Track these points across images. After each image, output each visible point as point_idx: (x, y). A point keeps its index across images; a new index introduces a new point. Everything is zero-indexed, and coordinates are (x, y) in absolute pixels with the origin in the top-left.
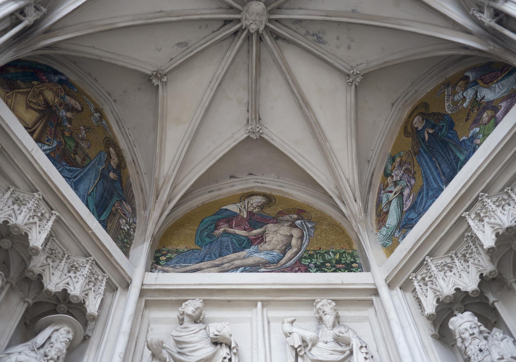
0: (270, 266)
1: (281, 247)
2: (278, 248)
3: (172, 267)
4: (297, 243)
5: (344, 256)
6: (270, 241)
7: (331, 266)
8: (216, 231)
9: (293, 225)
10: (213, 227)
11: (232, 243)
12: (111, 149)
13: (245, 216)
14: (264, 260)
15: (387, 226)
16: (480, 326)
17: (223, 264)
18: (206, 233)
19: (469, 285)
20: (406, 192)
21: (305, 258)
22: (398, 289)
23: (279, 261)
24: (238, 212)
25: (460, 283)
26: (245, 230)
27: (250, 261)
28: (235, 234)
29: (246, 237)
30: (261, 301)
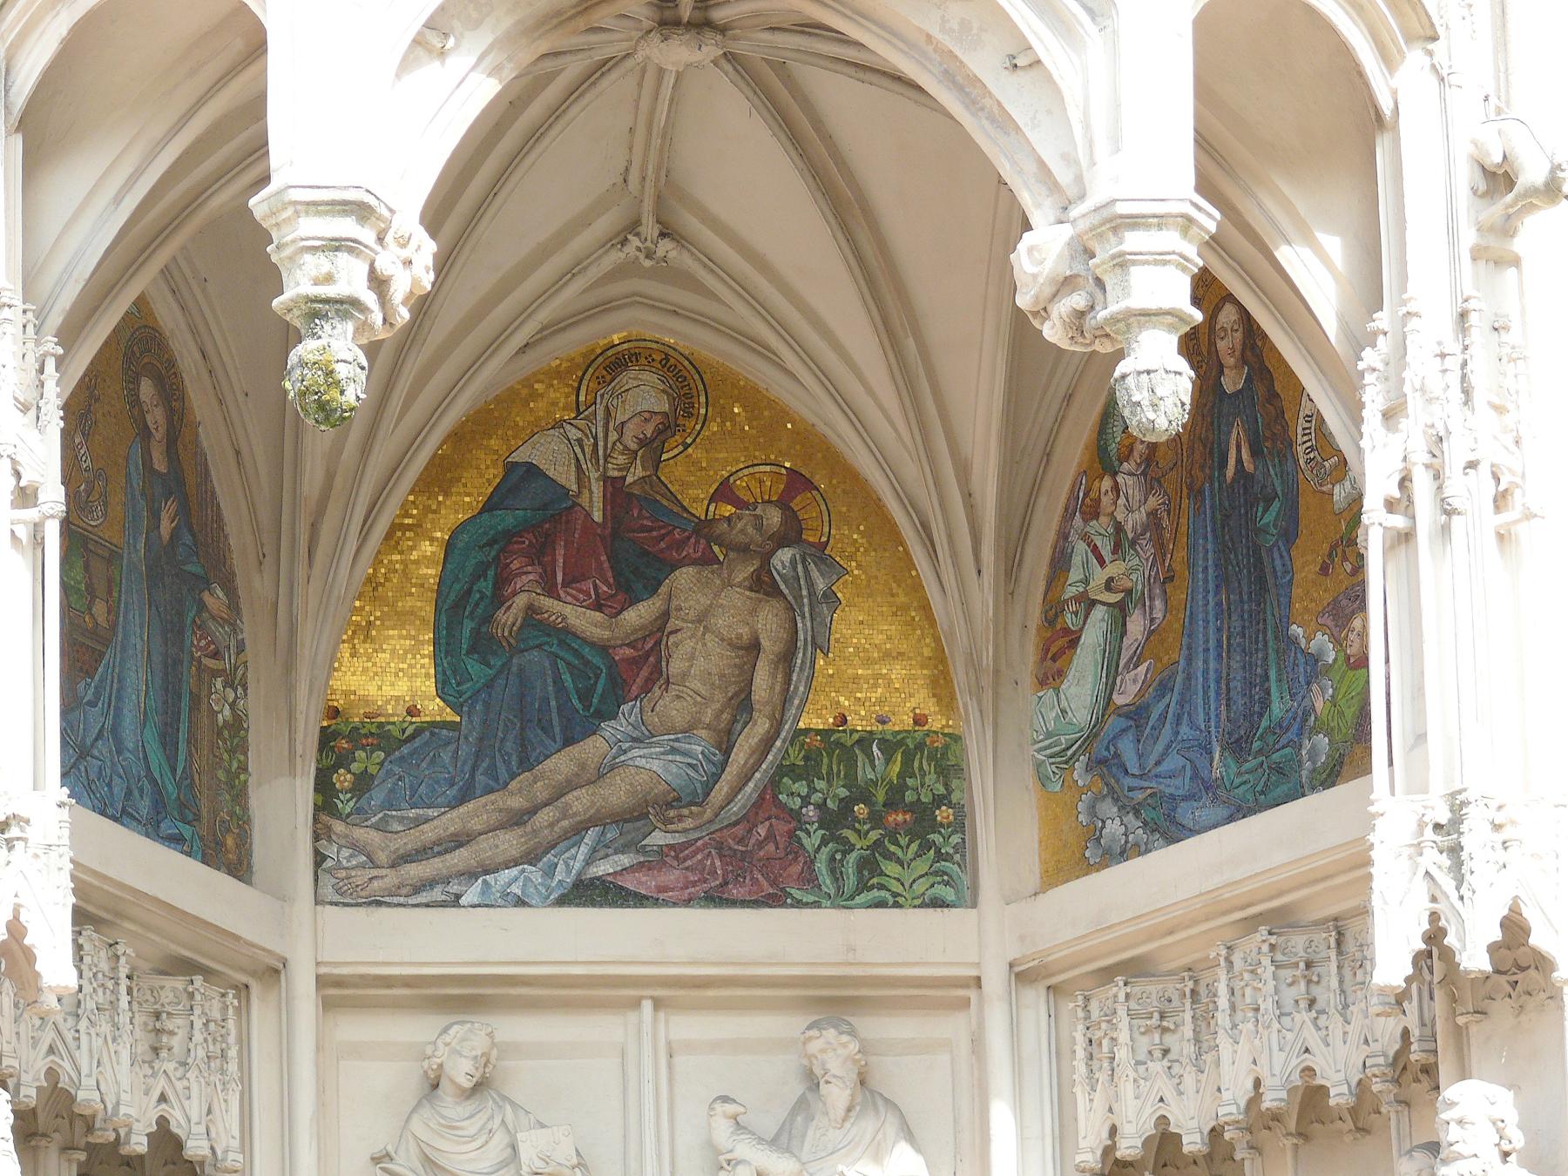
0: (681, 818)
1: (717, 716)
3: (376, 827)
4: (772, 688)
6: (685, 675)
8: (501, 616)
9: (763, 584)
10: (486, 586)
11: (558, 680)
12: (147, 389)
13: (597, 516)
14: (663, 787)
17: (533, 811)
18: (468, 626)
20: (1136, 626)
22: (1043, 991)
23: (708, 789)
26: (598, 607)
27: (615, 793)
28: (565, 635)
29: (603, 649)
30: (652, 998)
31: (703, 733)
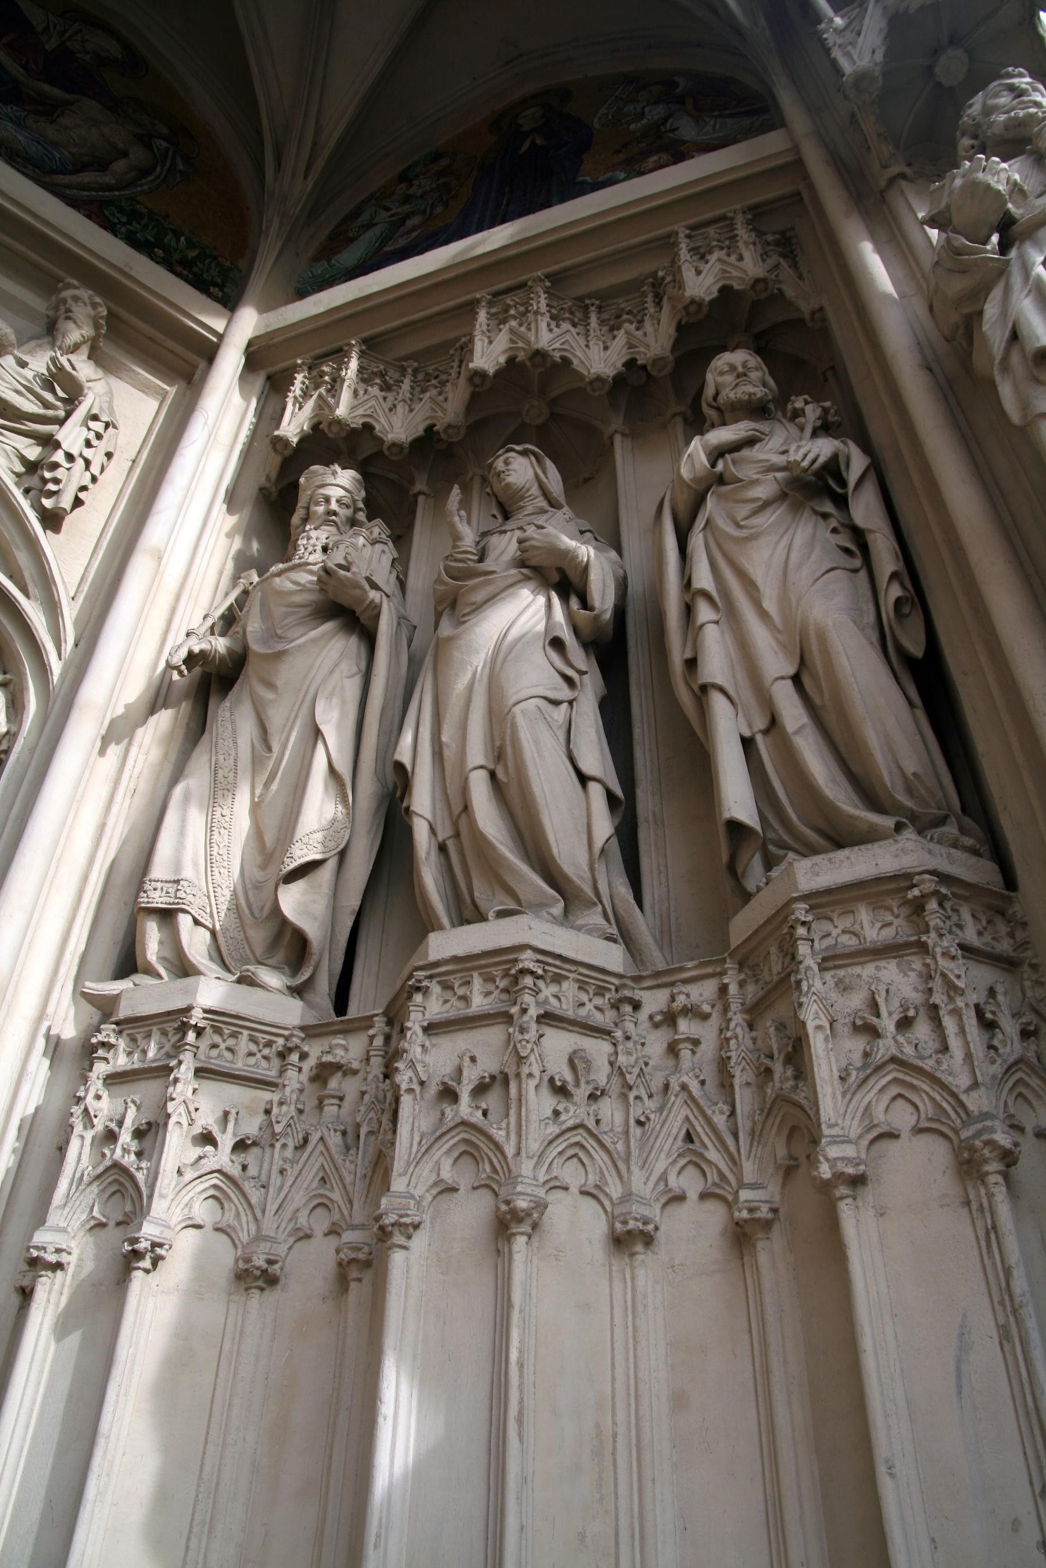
0: (25, 167)
2: (74, 150)
5: (207, 262)
7: (163, 259)
9: (145, 140)
13: (49, 47)
15: (333, 262)
16: (360, 509)
19: (395, 430)
21: (121, 210)
24: (39, 28)
25: (382, 420)
31: (66, 153)
